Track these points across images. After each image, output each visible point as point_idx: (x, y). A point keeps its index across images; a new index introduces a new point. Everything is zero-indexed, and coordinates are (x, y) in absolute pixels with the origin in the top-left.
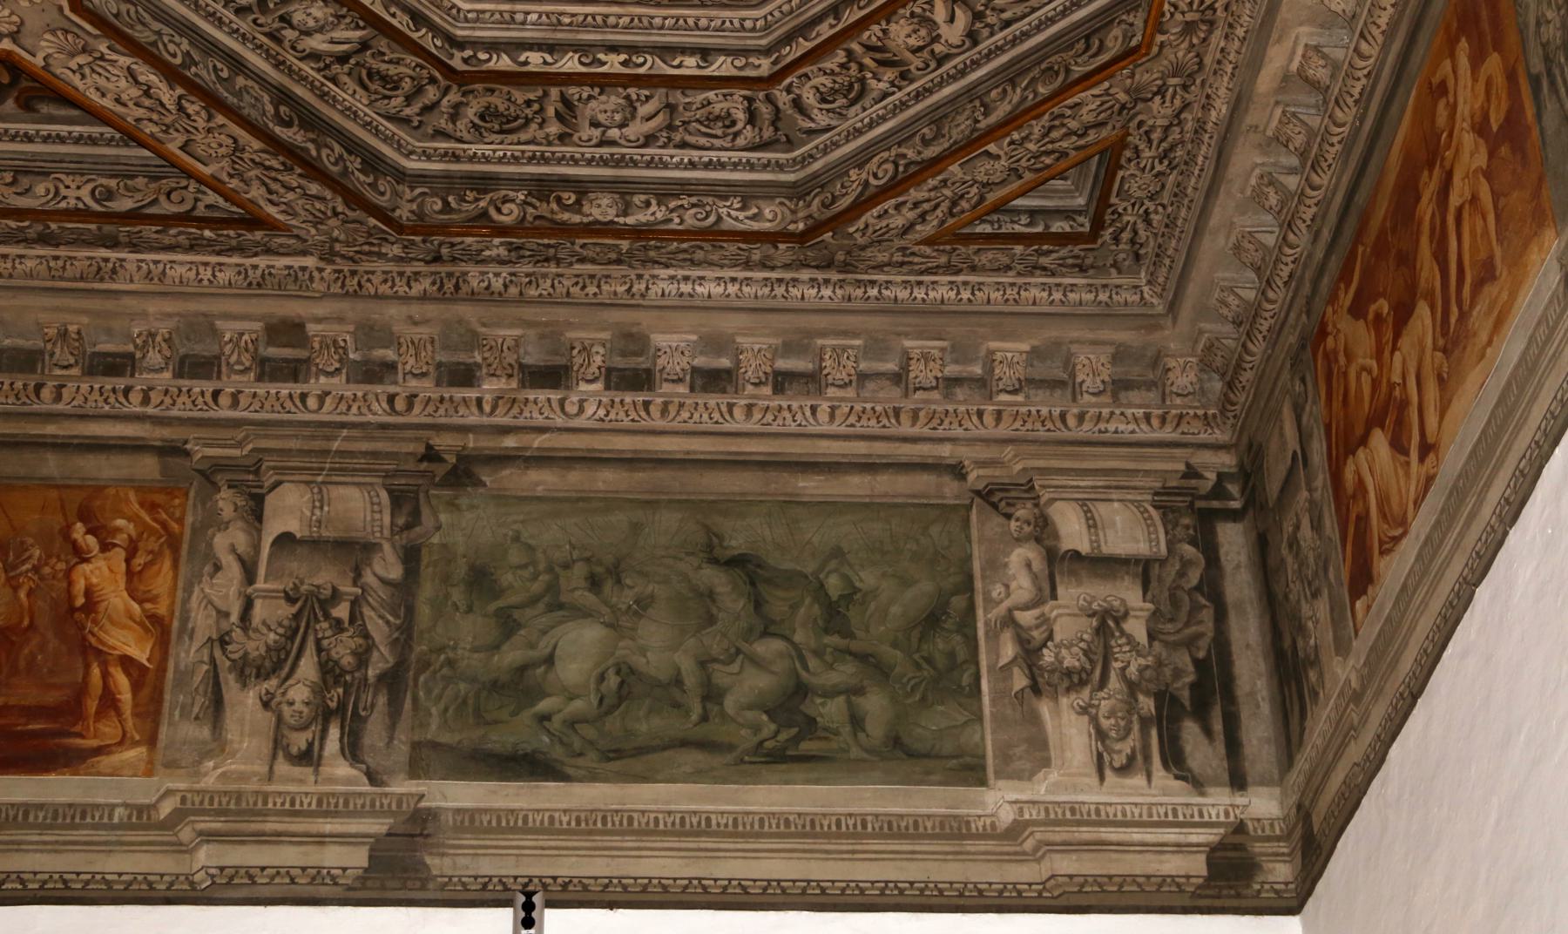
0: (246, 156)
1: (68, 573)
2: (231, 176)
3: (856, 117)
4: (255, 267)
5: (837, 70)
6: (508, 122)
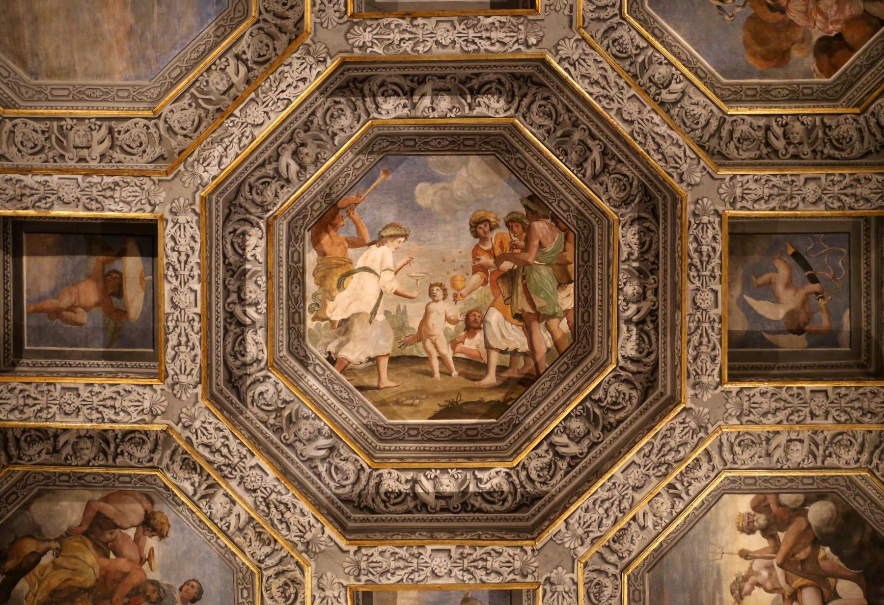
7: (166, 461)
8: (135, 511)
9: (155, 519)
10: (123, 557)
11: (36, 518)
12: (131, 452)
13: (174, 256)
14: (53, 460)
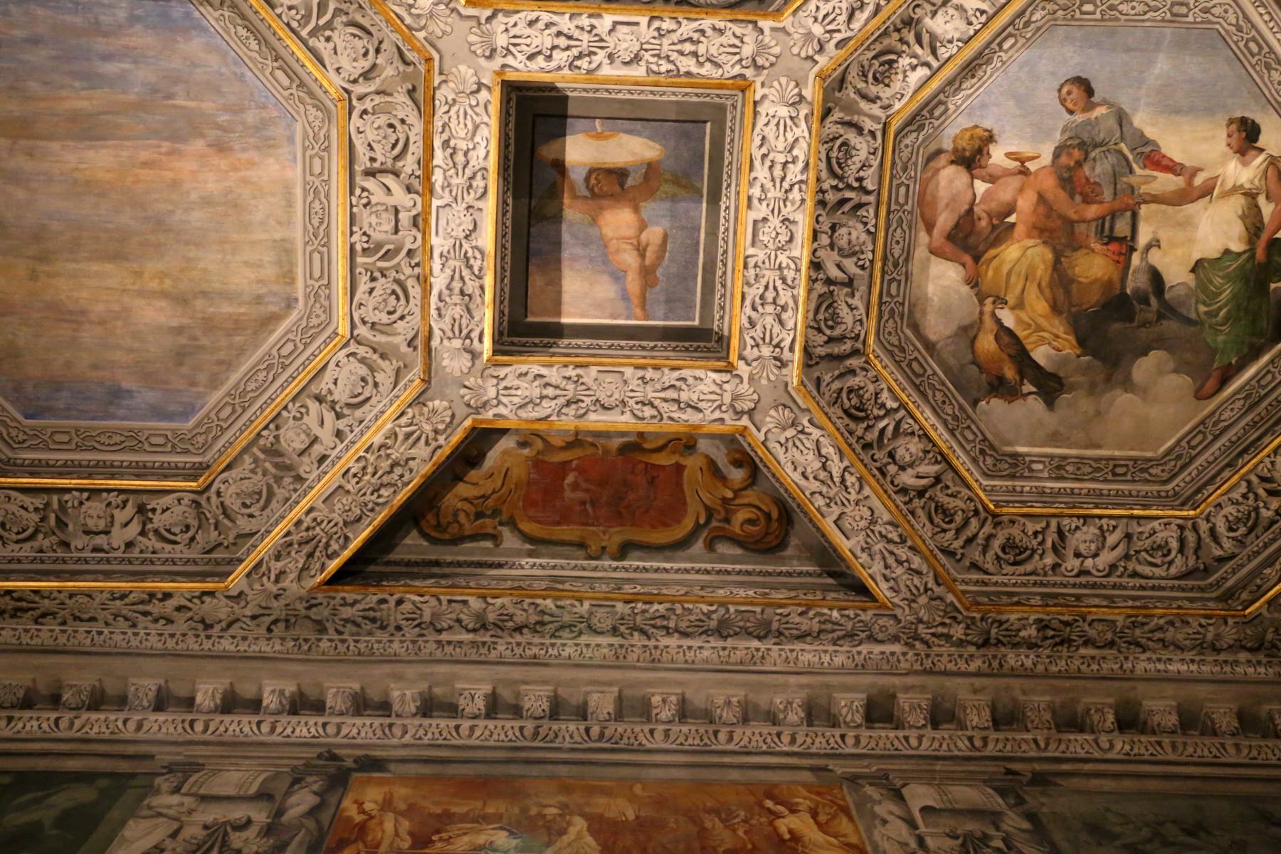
0: (877, 528)
1: (771, 823)
2: (863, 550)
3: (1254, 544)
4: (859, 653)
5: (1241, 500)
6: (1021, 553)
7: (875, 110)
8: (950, 179)
9: (964, 150)
10: (1015, 201)
11: (948, 333)
12: (859, 165)
13: (560, 57)
14: (863, 288)
